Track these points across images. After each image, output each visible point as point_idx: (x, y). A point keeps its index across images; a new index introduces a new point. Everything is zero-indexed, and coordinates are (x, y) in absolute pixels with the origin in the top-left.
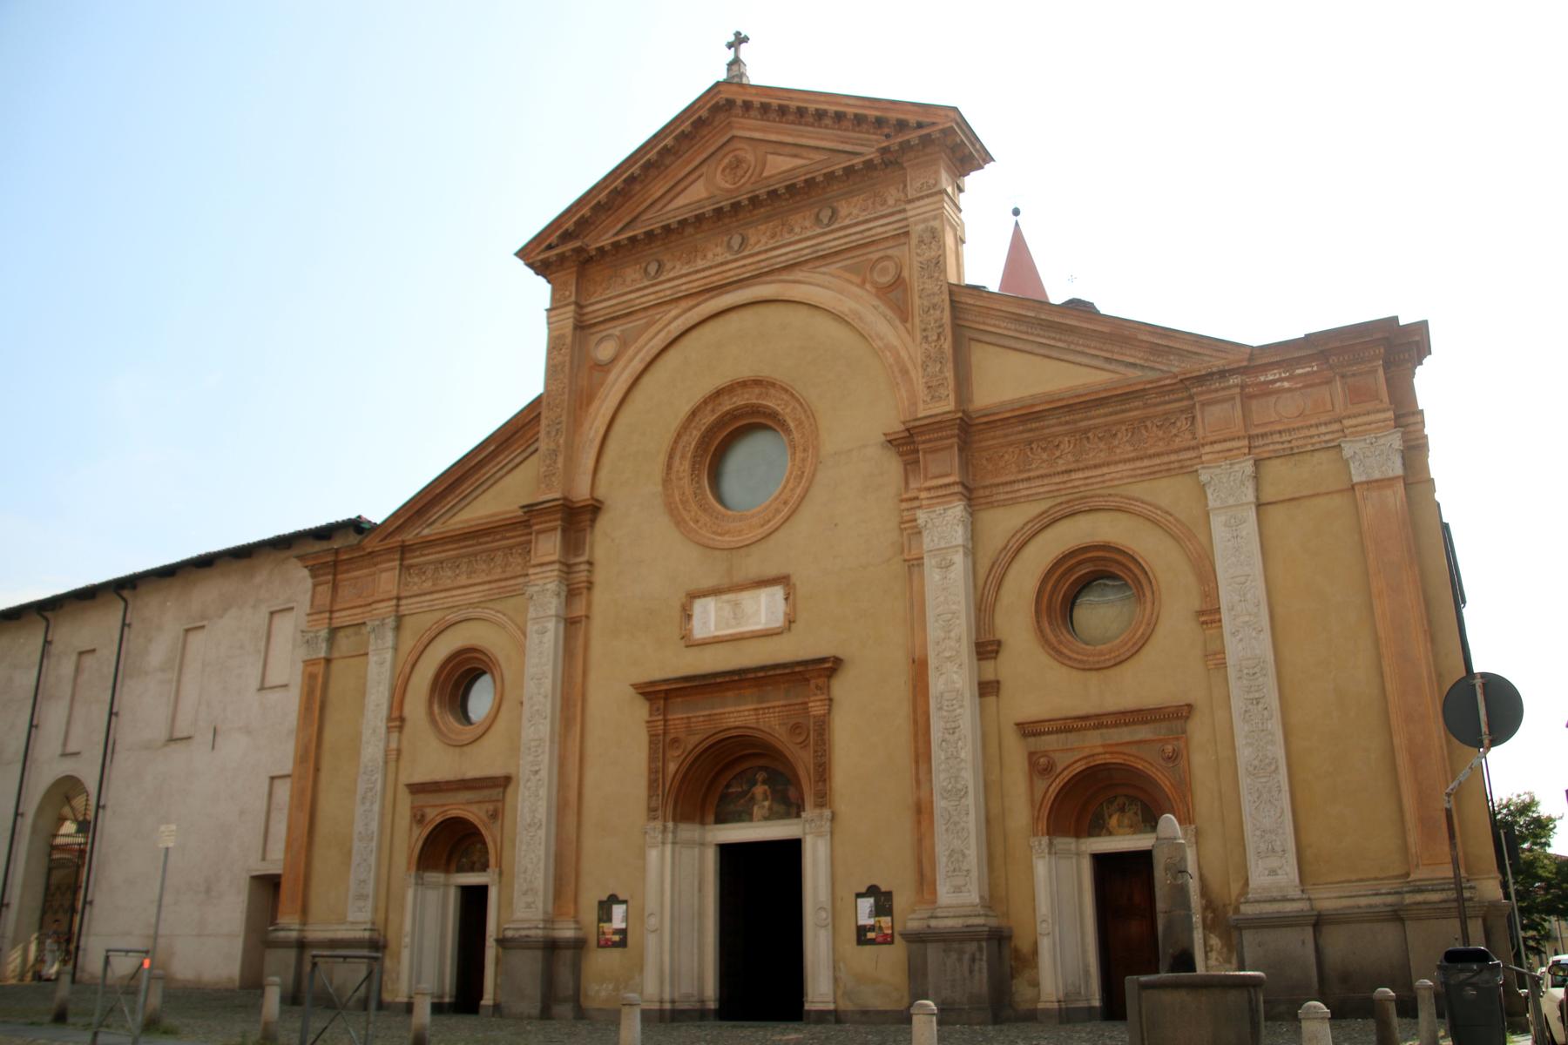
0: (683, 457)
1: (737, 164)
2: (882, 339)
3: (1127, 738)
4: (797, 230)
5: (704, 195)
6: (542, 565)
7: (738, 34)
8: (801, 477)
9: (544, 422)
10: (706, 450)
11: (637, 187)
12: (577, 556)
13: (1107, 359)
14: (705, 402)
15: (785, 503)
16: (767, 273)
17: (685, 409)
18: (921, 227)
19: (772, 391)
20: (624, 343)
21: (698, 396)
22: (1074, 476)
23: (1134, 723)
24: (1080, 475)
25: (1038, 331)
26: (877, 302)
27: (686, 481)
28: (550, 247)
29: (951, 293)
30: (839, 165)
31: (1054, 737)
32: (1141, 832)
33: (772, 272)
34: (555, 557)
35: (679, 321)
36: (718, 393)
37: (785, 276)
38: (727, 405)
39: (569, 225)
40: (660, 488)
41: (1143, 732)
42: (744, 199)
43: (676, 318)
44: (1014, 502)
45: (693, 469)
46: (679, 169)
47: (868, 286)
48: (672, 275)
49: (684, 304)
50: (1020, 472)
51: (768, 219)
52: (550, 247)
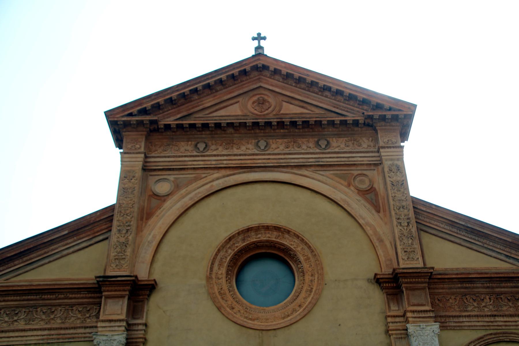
0: (220, 265)
1: (262, 102)
2: (363, 219)
4: (304, 147)
5: (239, 113)
6: (110, 321)
7: (259, 34)
8: (311, 291)
9: (115, 223)
10: (235, 264)
11: (196, 97)
12: (134, 318)
13: (507, 256)
14: (239, 234)
15: (300, 306)
16: (283, 167)
17: (224, 235)
18: (390, 162)
19: (287, 236)
20: (177, 187)
21: (233, 229)
22: (497, 319)
24: (501, 319)
25: (464, 233)
26: (359, 198)
27: (224, 280)
28: (131, 115)
29: (413, 202)
30: (337, 119)
33: (287, 166)
34: (123, 317)
35: (220, 181)
36: (249, 230)
37: (295, 171)
38: (253, 238)
39: (148, 105)
40: (204, 282)
42: (274, 121)
43: (218, 179)
44: (461, 328)
45: (227, 274)
46: (223, 95)
47: (352, 188)
48: (215, 153)
49: (224, 172)
50: (461, 311)
51: (284, 136)
52: (131, 115)
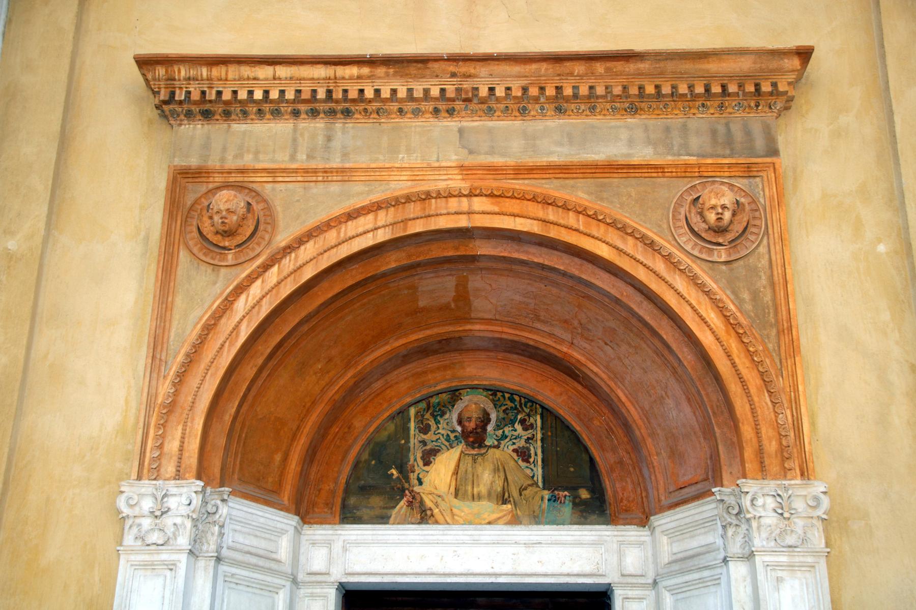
3: (559, 154)
23: (591, 102)
31: (282, 128)
32: (537, 519)
41: (620, 139)
